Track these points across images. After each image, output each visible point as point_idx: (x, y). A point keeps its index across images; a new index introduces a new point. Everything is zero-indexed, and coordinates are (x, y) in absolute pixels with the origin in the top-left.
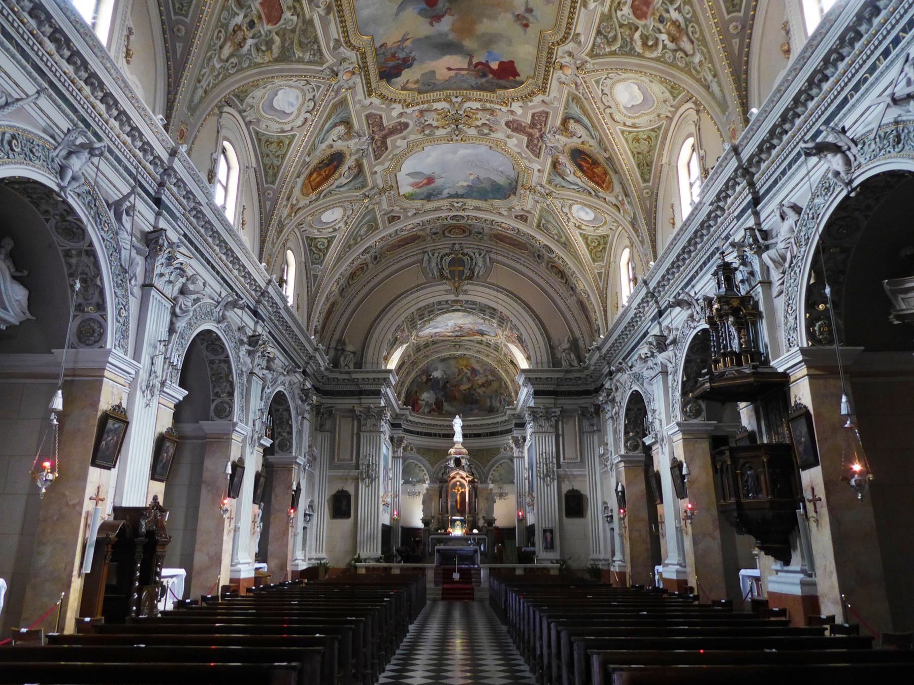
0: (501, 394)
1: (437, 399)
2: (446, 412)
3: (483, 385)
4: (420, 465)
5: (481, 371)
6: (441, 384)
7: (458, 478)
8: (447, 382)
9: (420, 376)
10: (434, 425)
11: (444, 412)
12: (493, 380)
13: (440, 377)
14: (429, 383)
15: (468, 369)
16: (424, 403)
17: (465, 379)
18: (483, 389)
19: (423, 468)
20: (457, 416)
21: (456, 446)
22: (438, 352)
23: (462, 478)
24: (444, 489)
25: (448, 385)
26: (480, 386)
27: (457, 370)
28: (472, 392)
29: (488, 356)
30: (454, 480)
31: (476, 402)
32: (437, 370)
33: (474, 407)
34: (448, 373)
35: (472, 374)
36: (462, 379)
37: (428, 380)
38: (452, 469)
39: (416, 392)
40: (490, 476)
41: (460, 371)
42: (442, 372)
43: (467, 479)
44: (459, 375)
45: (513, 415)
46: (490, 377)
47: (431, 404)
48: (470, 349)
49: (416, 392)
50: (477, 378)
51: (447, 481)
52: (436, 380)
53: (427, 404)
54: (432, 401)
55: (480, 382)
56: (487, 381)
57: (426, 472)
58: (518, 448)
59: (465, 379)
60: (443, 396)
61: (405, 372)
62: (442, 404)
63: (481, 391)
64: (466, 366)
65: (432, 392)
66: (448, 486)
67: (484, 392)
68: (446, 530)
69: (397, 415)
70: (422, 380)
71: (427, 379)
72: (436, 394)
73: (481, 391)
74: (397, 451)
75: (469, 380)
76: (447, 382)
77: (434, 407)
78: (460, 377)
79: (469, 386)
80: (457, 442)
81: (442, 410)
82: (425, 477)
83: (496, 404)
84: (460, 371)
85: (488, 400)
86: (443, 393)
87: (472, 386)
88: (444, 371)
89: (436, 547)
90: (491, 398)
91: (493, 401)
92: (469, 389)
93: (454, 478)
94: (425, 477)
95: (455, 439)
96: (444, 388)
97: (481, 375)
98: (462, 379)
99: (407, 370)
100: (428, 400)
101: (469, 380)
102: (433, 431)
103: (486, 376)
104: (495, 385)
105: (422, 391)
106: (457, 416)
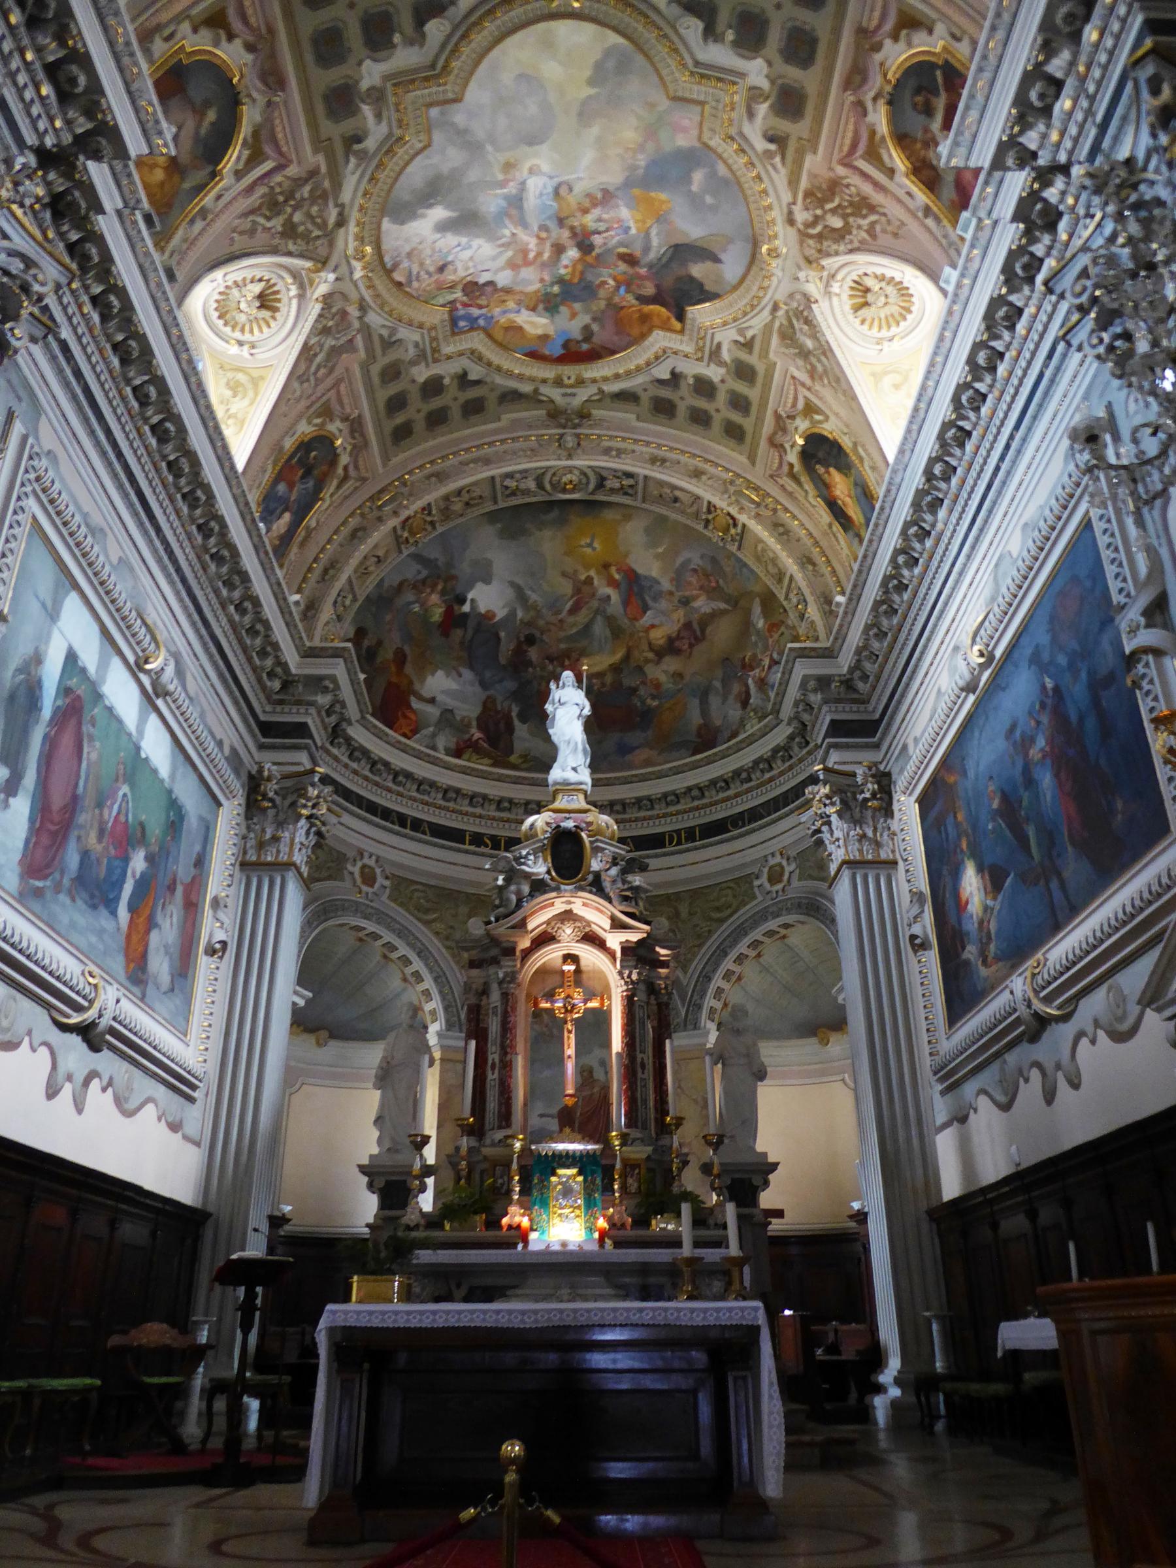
0: (747, 667)
1: (488, 706)
2: (525, 757)
3: (671, 648)
4: (403, 950)
5: (666, 585)
6: (507, 647)
7: (568, 941)
8: (531, 640)
9: (419, 586)
10: (472, 798)
11: (513, 759)
12: (714, 615)
13: (500, 614)
14: (458, 633)
15: (612, 583)
16: (433, 712)
17: (599, 628)
18: (671, 664)
19: (418, 965)
20: (568, 675)
21: (561, 802)
22: (487, 461)
23: (592, 939)
24: (495, 997)
25: (533, 654)
26: (660, 654)
27: (567, 588)
28: (629, 681)
29: (697, 474)
30: (550, 955)
31: (646, 717)
32: (487, 580)
33: (634, 737)
34: (534, 597)
35: (626, 603)
36: (587, 629)
37: (453, 620)
38: (539, 887)
39: (400, 658)
40: (710, 1002)
41: (582, 590)
42: (510, 593)
43: (615, 941)
44: (574, 610)
45: (823, 682)
46: (703, 605)
47: (464, 726)
48: (620, 452)
49: (400, 658)
50: (648, 619)
51: (510, 951)
52: (484, 624)
53: (447, 718)
54: (469, 710)
55: (658, 636)
56: (688, 626)
57: (428, 983)
58: (857, 822)
59: (599, 628)
60: (515, 696)
61: (345, 531)
62: (510, 729)
63: (661, 672)
64: (606, 566)
65: (467, 674)
66: (512, 977)
67: (678, 676)
68: (493, 1223)
69: (288, 683)
70: (426, 611)
71: (449, 613)
72: (484, 685)
73: (661, 672)
74: (275, 839)
75: (617, 632)
76: (531, 640)
77: (478, 735)
78: (582, 617)
79: (619, 656)
80: (567, 788)
81: (510, 750)
82: (428, 1007)
83: (725, 711)
84: (582, 590)
85: (694, 705)
86: (511, 685)
87: (627, 658)
88: (519, 590)
89: (334, 1315)
90: (704, 695)
91: (714, 701)
92: (616, 669)
93: (545, 939)
94: (428, 1007)
95: (556, 774)
96: (519, 662)
97: (663, 604)
98: (587, 629)
99: (353, 522)
100: (450, 703)
101: (617, 632)
102: (470, 826)
103: (685, 602)
104: (722, 634)
105: (426, 665)
106: (568, 675)
